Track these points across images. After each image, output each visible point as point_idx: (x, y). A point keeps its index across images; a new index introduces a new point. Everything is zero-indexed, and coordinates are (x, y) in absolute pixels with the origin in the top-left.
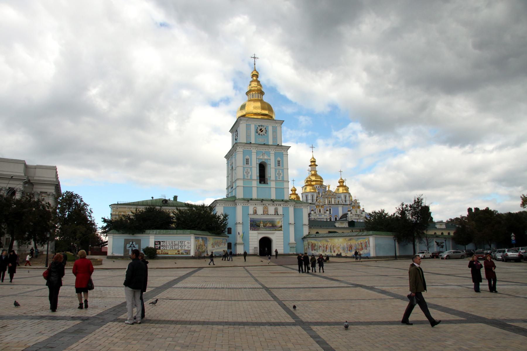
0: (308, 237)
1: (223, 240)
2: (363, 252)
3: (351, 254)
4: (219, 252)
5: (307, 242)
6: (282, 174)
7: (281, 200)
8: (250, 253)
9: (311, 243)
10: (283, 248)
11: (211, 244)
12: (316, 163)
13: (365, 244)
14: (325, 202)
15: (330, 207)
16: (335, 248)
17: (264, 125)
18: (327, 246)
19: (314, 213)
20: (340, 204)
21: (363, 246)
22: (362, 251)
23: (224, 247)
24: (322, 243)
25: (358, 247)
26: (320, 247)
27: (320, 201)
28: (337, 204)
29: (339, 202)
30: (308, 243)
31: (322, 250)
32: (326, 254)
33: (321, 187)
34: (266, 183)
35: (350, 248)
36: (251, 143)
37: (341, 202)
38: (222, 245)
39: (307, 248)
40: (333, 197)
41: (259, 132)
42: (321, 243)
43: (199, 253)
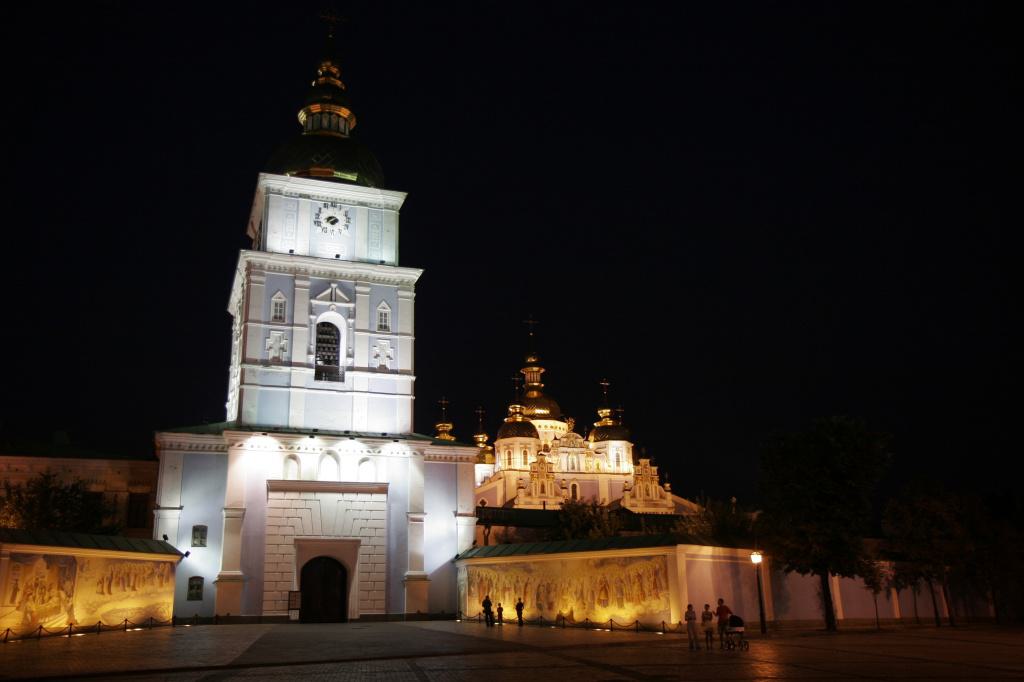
0: (470, 555)
1: (158, 567)
2: (646, 608)
8: (264, 614)
10: (384, 593)
11: (98, 577)
13: (652, 579)
15: (574, 479)
18: (529, 586)
22: (643, 603)
35: (603, 593)
38: (153, 584)
39: (465, 595)
41: (328, 225)
42: (509, 578)
43: (25, 618)
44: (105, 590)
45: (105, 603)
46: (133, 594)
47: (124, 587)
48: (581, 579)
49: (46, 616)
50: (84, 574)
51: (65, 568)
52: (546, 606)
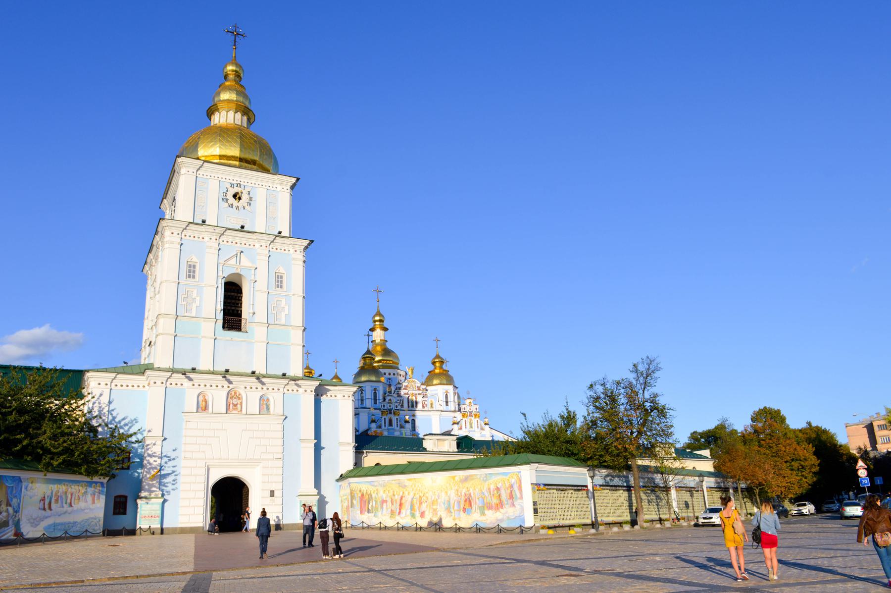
3: (470, 522)
4: (71, 523)
5: (348, 491)
6: (287, 307)
7: (281, 376)
9: (360, 491)
12: (386, 324)
13: (509, 491)
14: (402, 406)
16: (424, 505)
17: (246, 184)
18: (404, 498)
19: (377, 428)
20: (434, 409)
21: (504, 497)
22: (501, 510)
23: (92, 507)
24: (389, 491)
25: (488, 500)
26: (384, 502)
27: (390, 400)
28: (430, 410)
29: (434, 406)
30: (351, 493)
31: (390, 510)
32: (398, 523)
33: (394, 374)
34: (243, 329)
36: (204, 221)
37: (437, 406)
39: (348, 508)
40: (420, 394)
41: (232, 200)
42: (387, 492)
44: (47, 507)
45: (46, 518)
46: (71, 509)
47: (62, 503)
48: (449, 492)
50: (28, 493)
51: (13, 487)
52: (420, 515)
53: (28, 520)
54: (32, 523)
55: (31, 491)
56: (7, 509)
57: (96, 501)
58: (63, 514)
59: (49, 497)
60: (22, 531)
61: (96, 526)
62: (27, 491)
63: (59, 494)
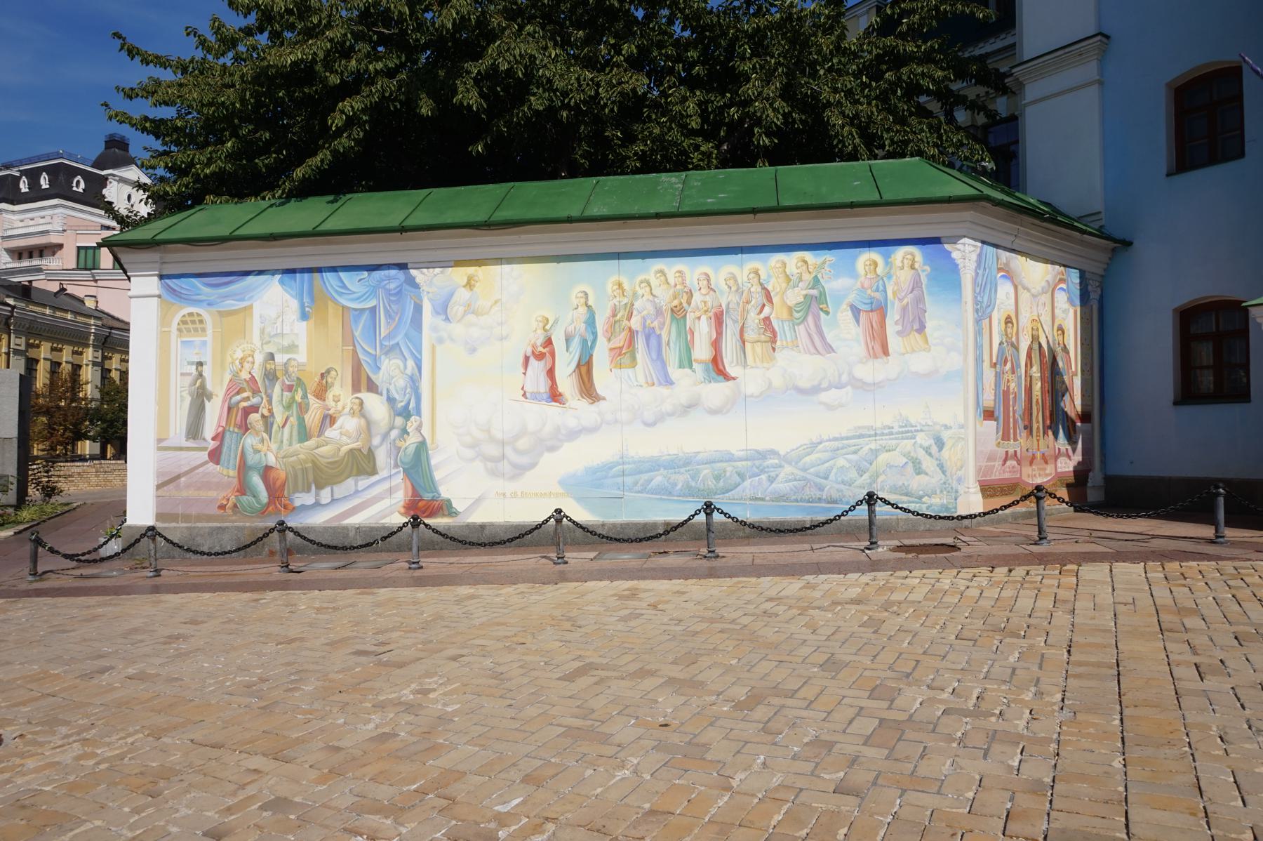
4: (730, 458)
11: (525, 336)
44: (566, 382)
45: (573, 435)
46: (717, 391)
49: (320, 487)
50: (457, 329)
51: (373, 310)
53: (473, 446)
54: (487, 459)
55: (471, 318)
56: (362, 403)
57: (893, 341)
58: (671, 414)
59: (576, 344)
60: (445, 492)
61: (919, 471)
62: (447, 319)
63: (635, 323)
